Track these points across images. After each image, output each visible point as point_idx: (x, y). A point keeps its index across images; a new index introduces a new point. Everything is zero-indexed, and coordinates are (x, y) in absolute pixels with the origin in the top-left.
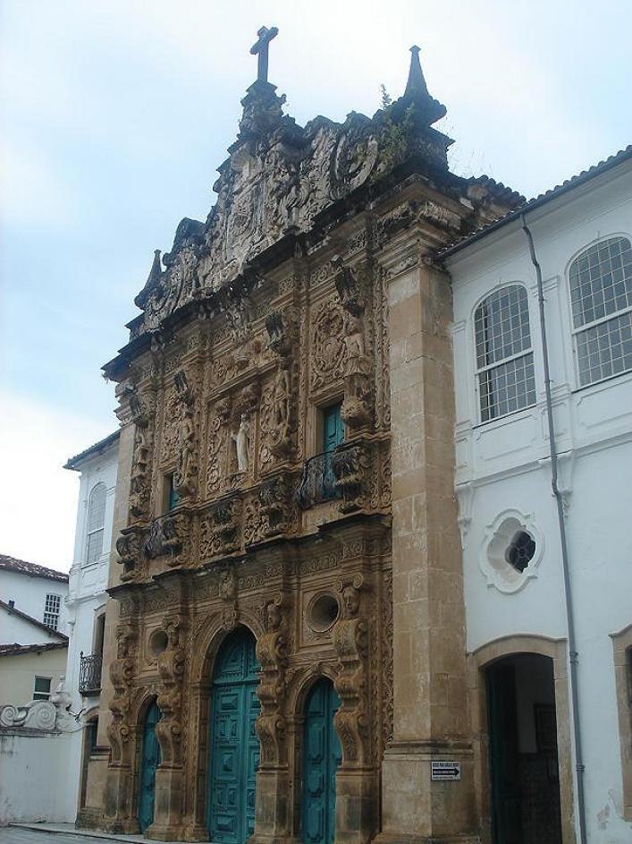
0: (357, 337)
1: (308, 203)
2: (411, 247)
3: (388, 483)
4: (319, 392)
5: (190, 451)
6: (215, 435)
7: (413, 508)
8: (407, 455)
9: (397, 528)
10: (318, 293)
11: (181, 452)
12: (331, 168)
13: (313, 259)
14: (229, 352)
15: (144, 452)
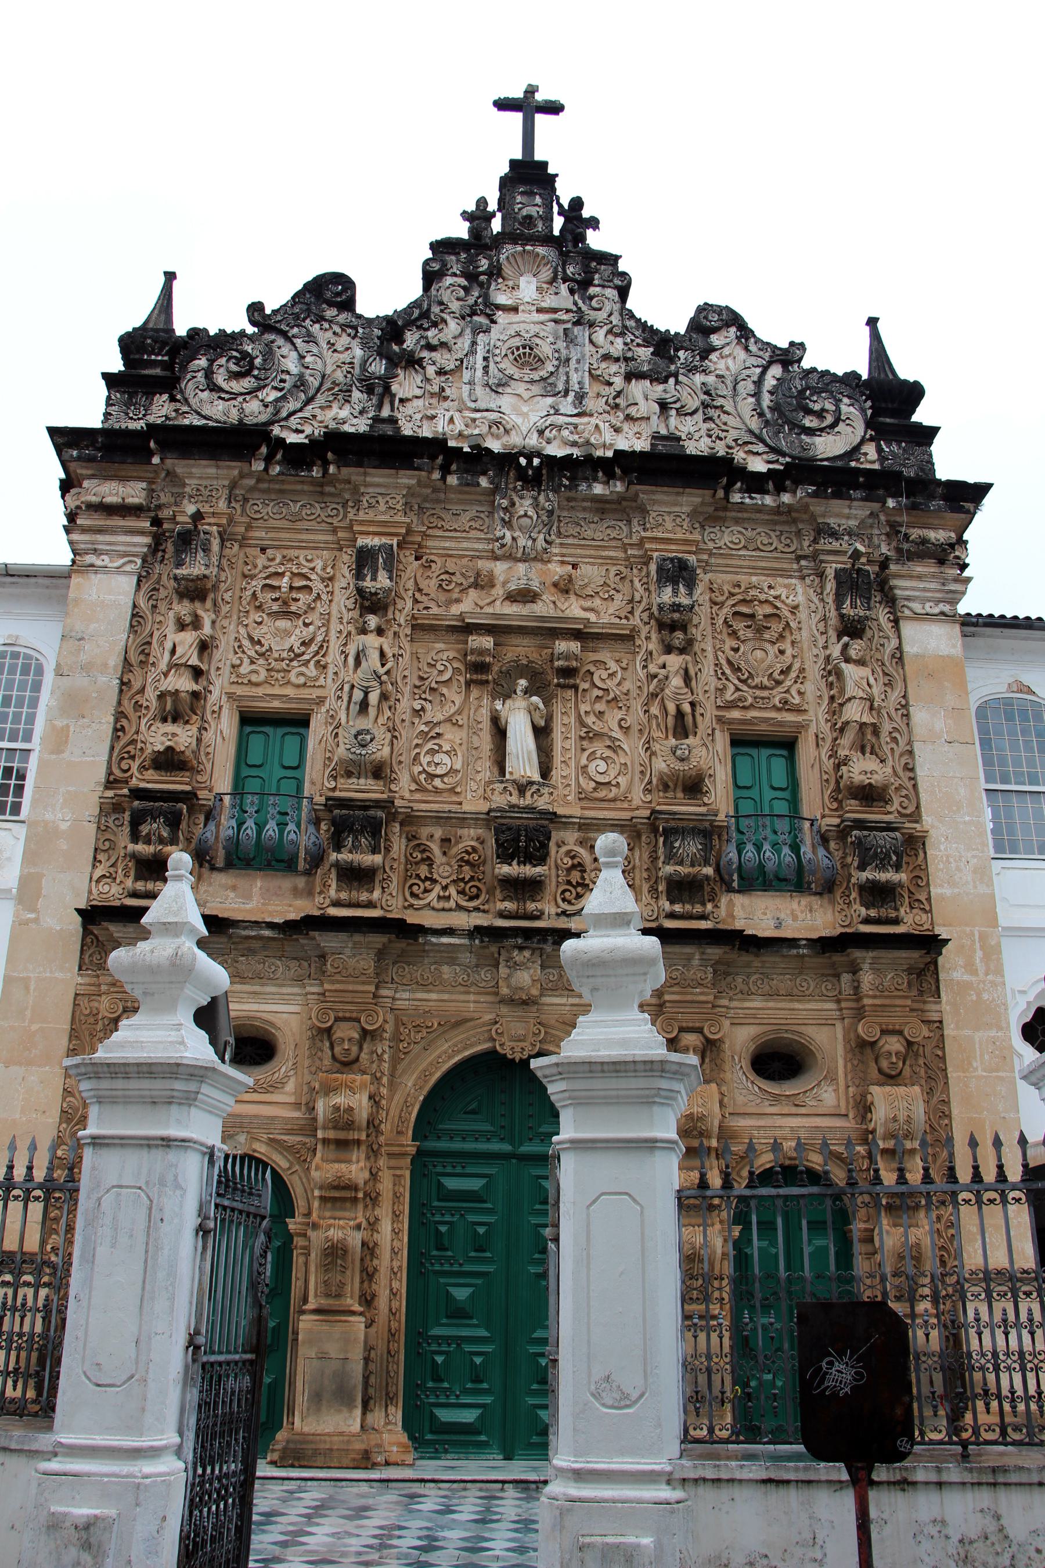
0: (864, 672)
1: (699, 416)
2: (951, 591)
3: (923, 897)
4: (736, 714)
5: (384, 697)
6: (432, 689)
7: (977, 945)
8: (958, 869)
9: (947, 966)
10: (729, 562)
11: (366, 694)
12: (757, 395)
13: (725, 509)
14: (473, 557)
15: (204, 647)
